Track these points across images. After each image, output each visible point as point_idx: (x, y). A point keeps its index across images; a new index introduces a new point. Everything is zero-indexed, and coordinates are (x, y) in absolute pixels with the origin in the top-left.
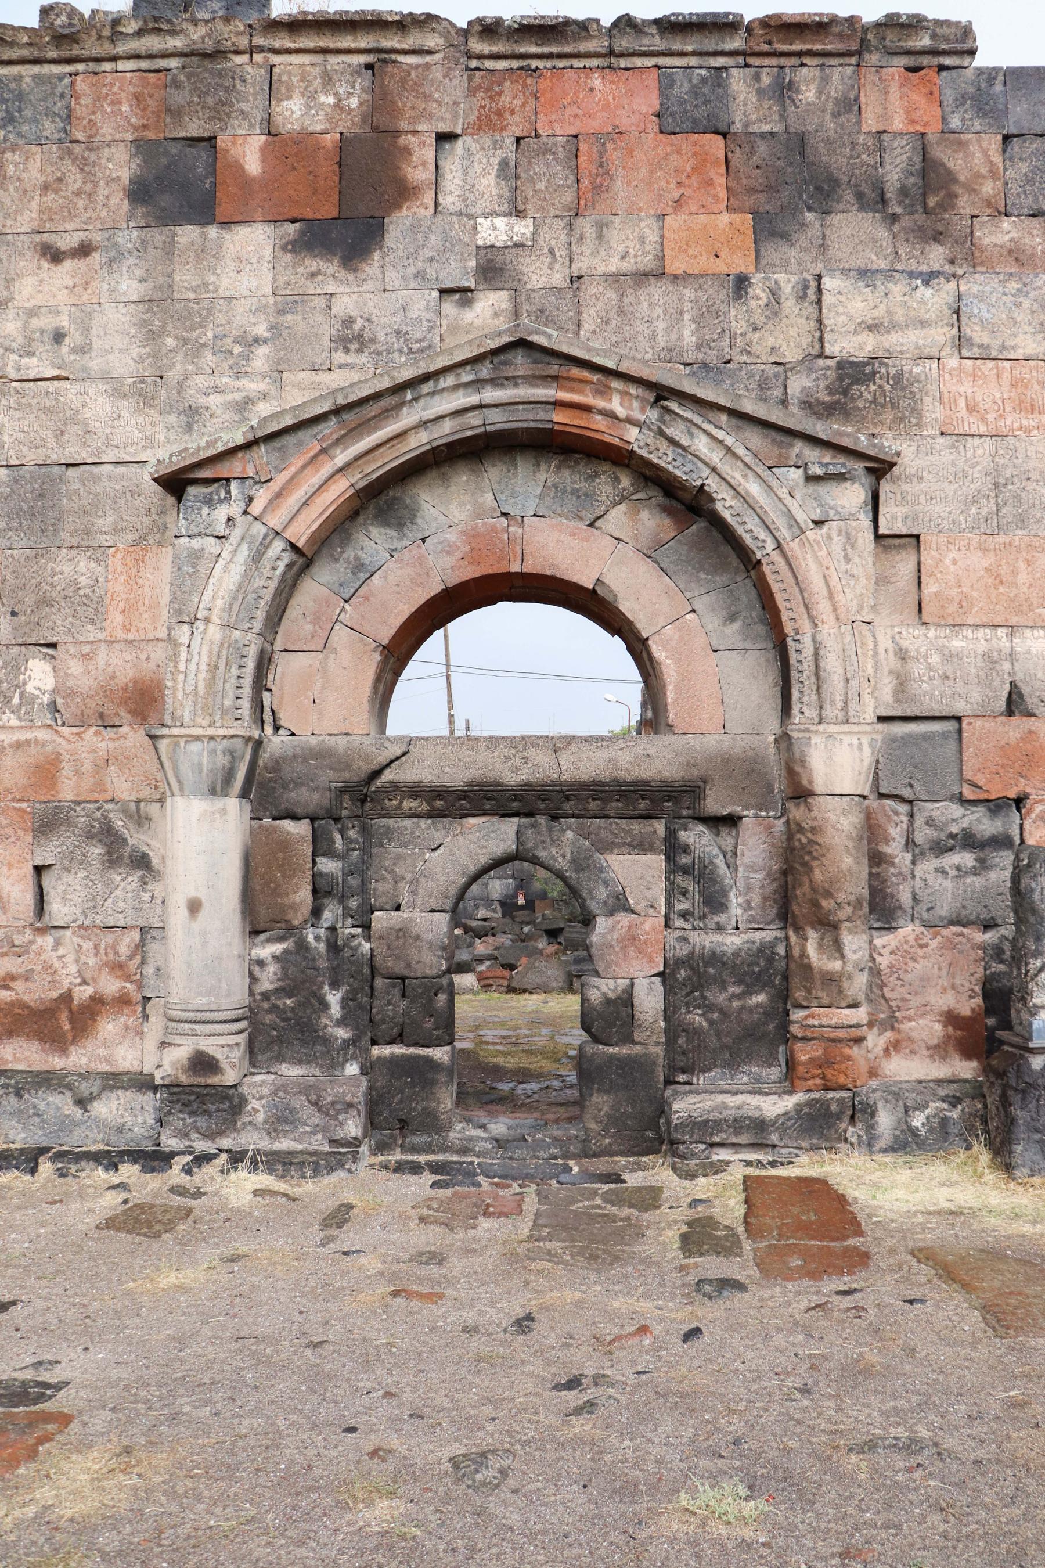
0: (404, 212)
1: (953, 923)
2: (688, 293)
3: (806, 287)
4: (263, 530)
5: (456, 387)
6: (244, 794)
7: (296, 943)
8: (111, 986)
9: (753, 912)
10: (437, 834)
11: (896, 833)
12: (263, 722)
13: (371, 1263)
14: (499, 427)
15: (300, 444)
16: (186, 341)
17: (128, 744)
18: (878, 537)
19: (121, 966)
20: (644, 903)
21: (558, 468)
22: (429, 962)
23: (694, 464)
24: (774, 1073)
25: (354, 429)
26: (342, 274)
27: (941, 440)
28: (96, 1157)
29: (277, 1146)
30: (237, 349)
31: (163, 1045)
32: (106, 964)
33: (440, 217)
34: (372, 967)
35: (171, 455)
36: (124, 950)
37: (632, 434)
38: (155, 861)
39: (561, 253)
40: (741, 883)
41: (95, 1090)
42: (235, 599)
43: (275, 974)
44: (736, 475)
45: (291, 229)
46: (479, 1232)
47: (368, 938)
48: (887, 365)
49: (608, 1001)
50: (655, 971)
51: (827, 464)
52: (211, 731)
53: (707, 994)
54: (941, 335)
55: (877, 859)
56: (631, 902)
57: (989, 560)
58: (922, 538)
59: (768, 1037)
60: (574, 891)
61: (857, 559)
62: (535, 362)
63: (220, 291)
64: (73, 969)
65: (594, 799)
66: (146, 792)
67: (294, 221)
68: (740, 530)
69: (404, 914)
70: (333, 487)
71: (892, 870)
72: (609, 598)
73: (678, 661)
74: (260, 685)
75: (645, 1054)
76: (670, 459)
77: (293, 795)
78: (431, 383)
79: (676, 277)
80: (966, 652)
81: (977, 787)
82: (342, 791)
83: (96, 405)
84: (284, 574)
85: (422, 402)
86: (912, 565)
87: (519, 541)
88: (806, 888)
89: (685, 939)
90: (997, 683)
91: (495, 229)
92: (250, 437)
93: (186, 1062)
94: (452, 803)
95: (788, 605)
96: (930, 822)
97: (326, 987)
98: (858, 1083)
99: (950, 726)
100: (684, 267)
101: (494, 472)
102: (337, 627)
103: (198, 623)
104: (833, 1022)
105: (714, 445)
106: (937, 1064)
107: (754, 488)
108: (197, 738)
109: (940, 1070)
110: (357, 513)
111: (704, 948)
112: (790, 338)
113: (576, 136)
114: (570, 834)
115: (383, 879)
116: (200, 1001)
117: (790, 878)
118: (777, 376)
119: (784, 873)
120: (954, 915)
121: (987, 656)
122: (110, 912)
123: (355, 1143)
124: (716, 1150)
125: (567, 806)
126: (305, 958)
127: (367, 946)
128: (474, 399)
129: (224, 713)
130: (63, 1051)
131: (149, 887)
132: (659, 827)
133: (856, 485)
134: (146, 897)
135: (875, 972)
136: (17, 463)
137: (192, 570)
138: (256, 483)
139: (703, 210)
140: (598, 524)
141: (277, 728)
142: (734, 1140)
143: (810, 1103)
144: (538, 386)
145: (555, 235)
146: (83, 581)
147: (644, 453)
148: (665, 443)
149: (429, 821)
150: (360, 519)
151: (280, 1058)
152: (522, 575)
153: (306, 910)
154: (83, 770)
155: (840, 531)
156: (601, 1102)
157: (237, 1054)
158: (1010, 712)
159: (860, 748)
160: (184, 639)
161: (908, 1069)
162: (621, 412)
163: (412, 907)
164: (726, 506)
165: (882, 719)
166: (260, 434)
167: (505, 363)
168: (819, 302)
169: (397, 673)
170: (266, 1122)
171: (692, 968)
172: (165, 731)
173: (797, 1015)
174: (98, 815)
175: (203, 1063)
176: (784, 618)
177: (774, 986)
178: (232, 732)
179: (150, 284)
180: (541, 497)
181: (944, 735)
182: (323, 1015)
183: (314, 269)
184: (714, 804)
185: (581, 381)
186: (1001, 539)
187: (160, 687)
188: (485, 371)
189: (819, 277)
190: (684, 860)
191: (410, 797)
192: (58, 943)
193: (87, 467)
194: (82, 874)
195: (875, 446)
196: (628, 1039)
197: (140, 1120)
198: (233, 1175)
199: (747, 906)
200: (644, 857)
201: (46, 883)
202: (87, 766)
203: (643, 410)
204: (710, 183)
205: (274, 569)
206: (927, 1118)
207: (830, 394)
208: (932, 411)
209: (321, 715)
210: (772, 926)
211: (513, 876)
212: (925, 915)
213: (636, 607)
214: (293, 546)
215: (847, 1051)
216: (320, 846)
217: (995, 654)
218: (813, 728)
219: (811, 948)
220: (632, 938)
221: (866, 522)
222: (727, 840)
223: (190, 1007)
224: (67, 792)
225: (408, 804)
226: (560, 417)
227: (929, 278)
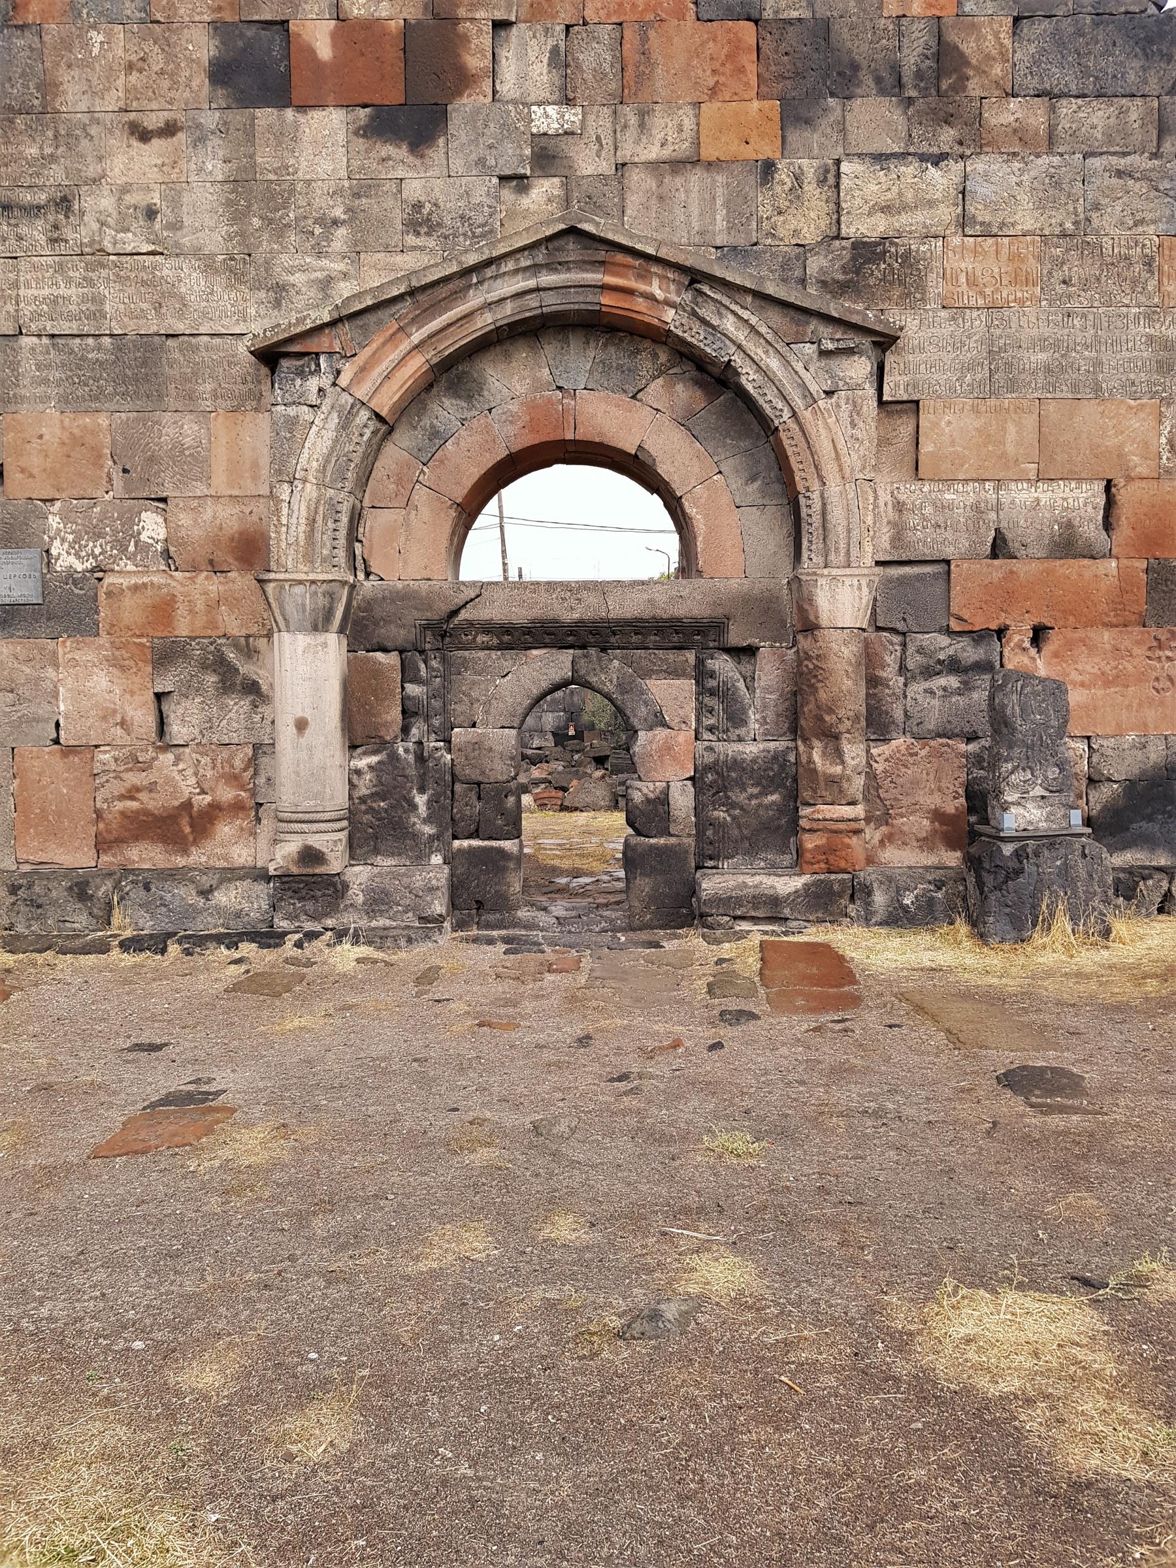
0: (465, 100)
1: (939, 736)
2: (720, 179)
3: (827, 171)
4: (351, 400)
5: (516, 271)
6: (341, 631)
8: (227, 794)
11: (891, 660)
12: (355, 569)
13: (459, 1007)
14: (554, 308)
15: (380, 323)
16: (271, 221)
17: (236, 587)
18: (881, 403)
19: (236, 777)
20: (677, 720)
21: (605, 345)
22: (499, 770)
23: (723, 342)
24: (787, 859)
25: (427, 309)
26: (410, 159)
27: (944, 314)
28: (219, 939)
29: (374, 924)
30: (318, 230)
31: (276, 842)
32: (222, 776)
33: (498, 105)
34: (453, 775)
35: (265, 330)
36: (238, 763)
37: (670, 315)
38: (264, 688)
39: (607, 141)
40: (758, 702)
41: (214, 883)
42: (327, 461)
43: (371, 781)
44: (758, 352)
45: (363, 113)
46: (545, 983)
47: (449, 751)
48: (897, 245)
49: (648, 801)
51: (838, 340)
52: (312, 577)
53: (730, 794)
54: (946, 213)
55: (873, 682)
57: (978, 424)
58: (921, 403)
59: (780, 833)
60: (619, 710)
61: (861, 425)
62: (585, 248)
63: (300, 174)
64: (192, 781)
65: (636, 634)
66: (254, 629)
67: (365, 106)
68: (761, 401)
70: (411, 362)
71: (887, 691)
72: (649, 462)
73: (706, 516)
74: (353, 537)
76: (701, 338)
78: (494, 267)
79: (710, 164)
81: (962, 620)
82: (425, 628)
83: (191, 281)
84: (370, 440)
85: (486, 285)
86: (911, 428)
87: (572, 412)
88: (811, 706)
91: (547, 116)
92: (336, 316)
93: (296, 856)
94: (518, 637)
95: (801, 467)
96: (920, 651)
98: (857, 868)
100: (716, 154)
101: (549, 349)
102: (417, 487)
103: (296, 482)
105: (740, 324)
107: (774, 363)
108: (300, 582)
109: (929, 860)
110: (431, 386)
112: (808, 222)
113: (620, 24)
114: (616, 663)
116: (308, 804)
117: (799, 697)
118: (797, 258)
119: (795, 694)
120: (940, 729)
121: (977, 508)
122: (225, 731)
123: (440, 919)
124: (738, 922)
125: (613, 640)
126: (397, 768)
127: (449, 757)
128: (531, 283)
129: (324, 560)
130: (185, 852)
131: (259, 710)
132: (691, 656)
133: (863, 358)
134: (257, 718)
135: (871, 775)
136: (120, 332)
137: (288, 436)
138: (342, 357)
139: (735, 98)
140: (639, 396)
141: (368, 574)
142: (754, 914)
143: (817, 883)
144: (587, 271)
145: (600, 122)
146: (188, 442)
147: (680, 334)
148: (698, 323)
149: (499, 653)
150: (435, 390)
151: (376, 851)
152: (575, 442)
153: (396, 728)
154: (197, 609)
155: (848, 399)
156: (644, 885)
157: (341, 847)
158: (994, 555)
159: (860, 588)
160: (285, 496)
161: (899, 858)
162: (659, 294)
164: (749, 379)
165: (878, 563)
166: (344, 312)
167: (557, 249)
168: (837, 186)
169: (468, 527)
170: (364, 904)
171: (717, 773)
172: (272, 576)
173: (805, 811)
174: (212, 648)
175: (310, 856)
177: (785, 787)
178: (330, 577)
179: (234, 165)
180: (590, 372)
181: (935, 576)
182: (412, 815)
183: (383, 154)
184: (735, 637)
185: (625, 266)
186: (992, 402)
187: (266, 538)
188: (541, 257)
189: (838, 162)
190: (712, 683)
191: (483, 632)
192: (178, 759)
193: (186, 338)
194: (198, 700)
195: (881, 321)
197: (256, 906)
198: (338, 948)
199: (763, 722)
200: (678, 682)
201: (165, 708)
202: (200, 606)
203: (678, 294)
204: (741, 70)
205: (361, 435)
206: (916, 897)
207: (845, 273)
208: (935, 286)
209: (405, 562)
212: (915, 729)
213: (672, 470)
214: (378, 416)
215: (847, 840)
216: (408, 674)
218: (819, 572)
219: (816, 756)
220: (668, 748)
221: (870, 391)
222: (747, 668)
223: (299, 809)
224: (183, 628)
225: (481, 638)
226: (606, 299)
227: (937, 160)
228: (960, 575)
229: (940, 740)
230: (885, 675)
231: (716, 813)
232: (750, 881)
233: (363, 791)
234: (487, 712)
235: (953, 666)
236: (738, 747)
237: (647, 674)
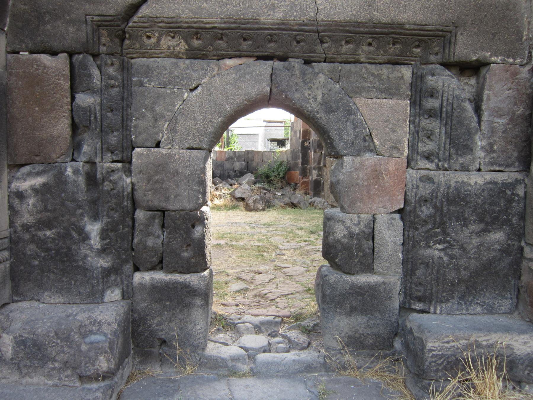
7: (55, 176)
9: (494, 155)
10: (195, 75)
47: (129, 172)
49: (351, 235)
50: (397, 208)
53: (449, 231)
56: (377, 143)
65: (347, 42)
69: (163, 151)
75: (384, 283)
77: (49, 27)
82: (98, 26)
89: (429, 180)
97: (86, 219)
114: (322, 78)
115: (143, 116)
127: (128, 180)
132: (406, 72)
149: (188, 61)
163: (171, 142)
171: (435, 207)
177: (512, 225)
184: (464, 49)
190: (432, 103)
196: (369, 269)
199: (489, 149)
200: (391, 102)
211: (244, 161)
225: (166, 42)
231: (429, 252)
233: (27, 218)
234: (173, 130)
237: (358, 92)
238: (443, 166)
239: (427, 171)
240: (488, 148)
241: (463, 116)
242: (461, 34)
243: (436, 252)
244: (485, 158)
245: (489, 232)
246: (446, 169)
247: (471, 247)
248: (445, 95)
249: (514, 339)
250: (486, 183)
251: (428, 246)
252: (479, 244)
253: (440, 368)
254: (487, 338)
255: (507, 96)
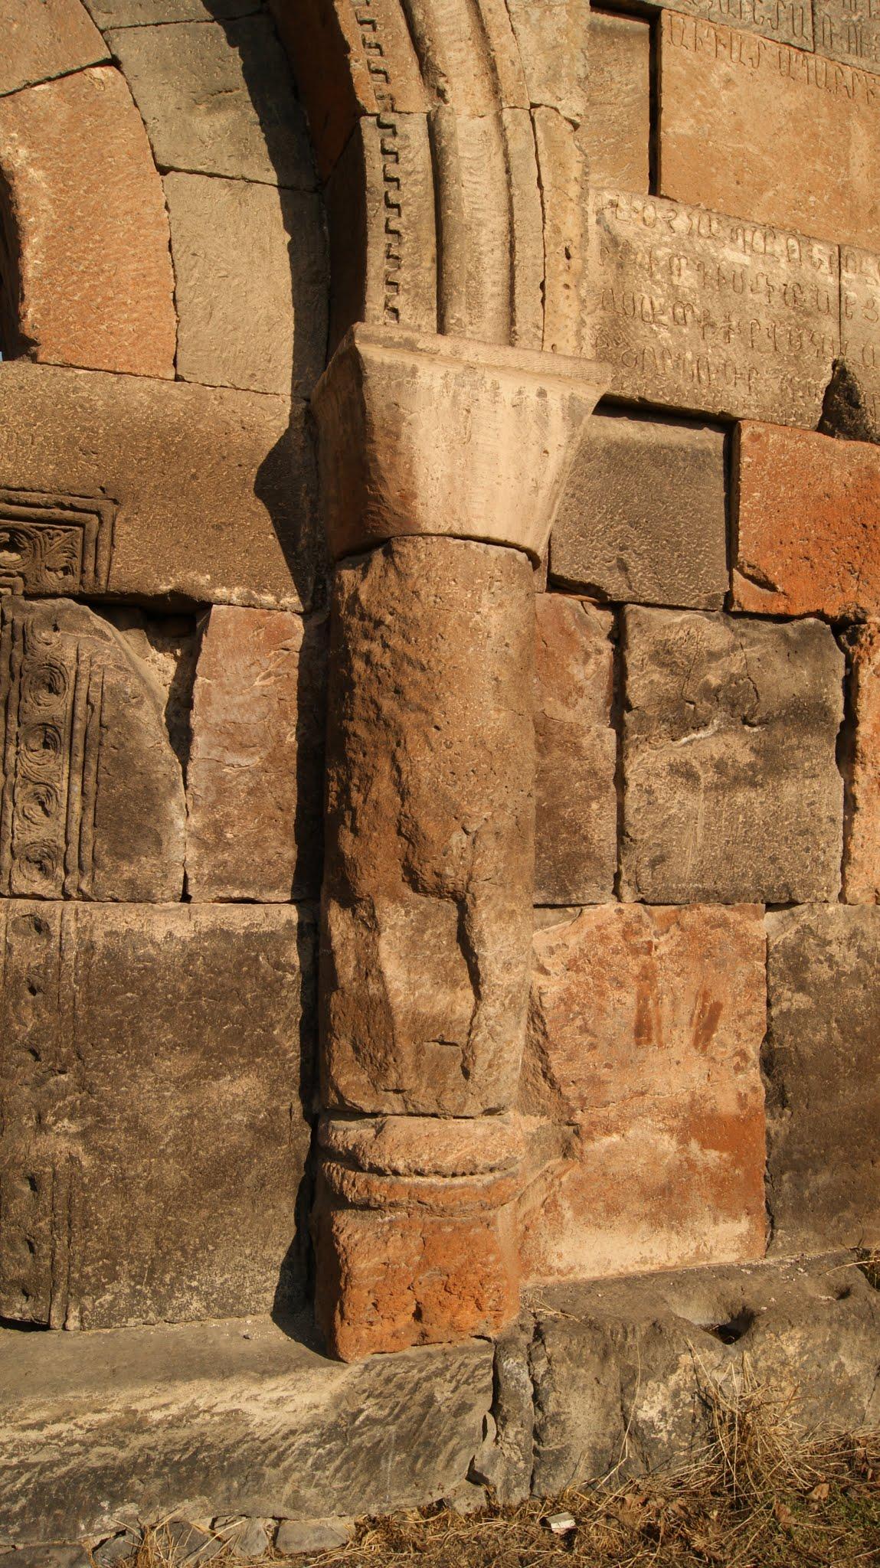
1: (707, 896)
11: (589, 672)
40: (197, 773)
53: (95, 1077)
58: (665, 17)
71: (574, 764)
80: (750, 276)
89: (40, 927)
90: (810, 356)
95: (371, 37)
96: (663, 655)
99: (711, 440)
104: (448, 1162)
106: (663, 1235)
111: (90, 948)
121: (792, 295)
159: (543, 421)
176: (357, 67)
186: (817, 62)
199: (212, 839)
210: (273, 896)
217: (808, 295)
228: (761, 461)
229: (707, 910)
230: (569, 716)
232: (162, 1403)
235: (739, 704)
236: (125, 918)
238: (79, 890)
239: (31, 903)
240: (209, 837)
241: (132, 744)
242: (127, 520)
243: (63, 1145)
244: (200, 864)
245: (217, 1077)
246: (86, 898)
247: (164, 1121)
248: (84, 684)
249: (246, 1394)
250: (199, 936)
251: (41, 1127)
252: (186, 1112)
253: (17, 1508)
254: (162, 1401)
255: (258, 694)
